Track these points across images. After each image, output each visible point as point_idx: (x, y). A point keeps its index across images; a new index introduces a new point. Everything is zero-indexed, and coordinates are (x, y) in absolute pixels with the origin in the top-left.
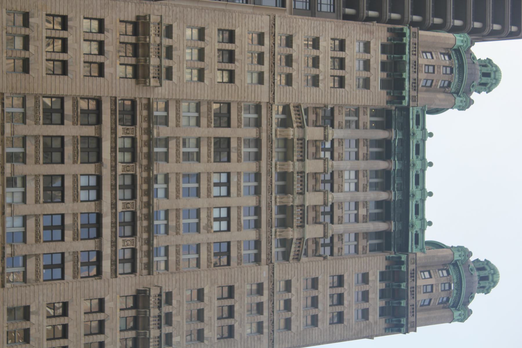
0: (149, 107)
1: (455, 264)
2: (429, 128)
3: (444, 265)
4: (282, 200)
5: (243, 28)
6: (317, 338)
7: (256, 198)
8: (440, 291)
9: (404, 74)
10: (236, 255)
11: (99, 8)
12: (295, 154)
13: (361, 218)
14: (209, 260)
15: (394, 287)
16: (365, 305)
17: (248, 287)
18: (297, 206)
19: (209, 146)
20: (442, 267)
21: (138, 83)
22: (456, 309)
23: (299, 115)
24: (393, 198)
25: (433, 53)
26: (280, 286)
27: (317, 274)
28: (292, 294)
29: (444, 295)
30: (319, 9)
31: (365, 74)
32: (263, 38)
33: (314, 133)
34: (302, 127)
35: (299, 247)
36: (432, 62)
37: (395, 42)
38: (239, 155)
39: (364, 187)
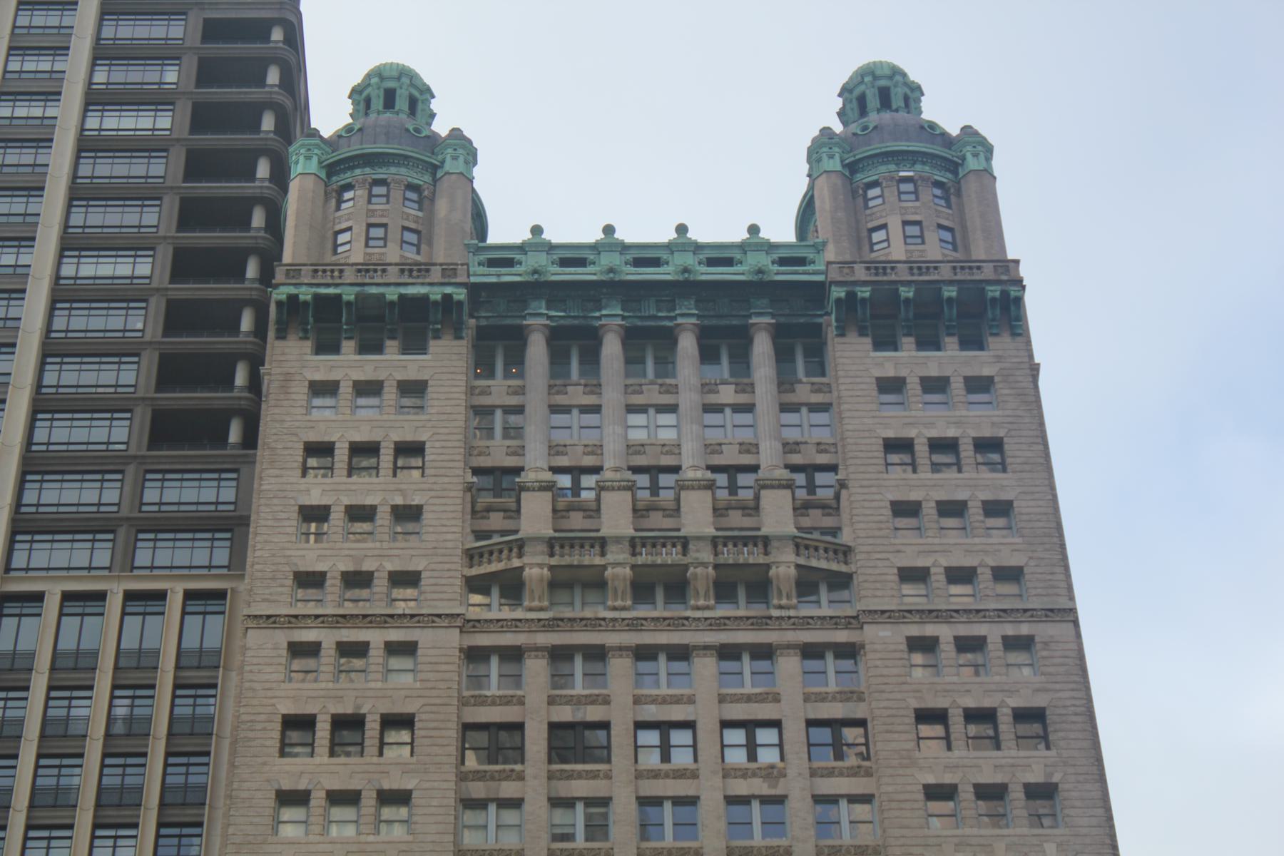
1: (852, 168)
2: (521, 235)
3: (854, 193)
4: (702, 593)
5: (278, 693)
6: (1040, 503)
7: (698, 656)
8: (917, 204)
9: (389, 297)
10: (840, 705)
12: (586, 561)
13: (743, 399)
14: (854, 772)
15: (911, 315)
16: (957, 385)
17: (918, 673)
18: (716, 555)
19: (570, 776)
20: (860, 201)
22: (962, 165)
23: (491, 553)
24: (694, 320)
25: (337, 228)
26: (913, 595)
27: (882, 504)
28: (934, 565)
29: (928, 193)
30: (231, 507)
31: (390, 393)
32: (301, 643)
33: (536, 517)
34: (520, 546)
35: (816, 549)
36: (359, 229)
37: (311, 320)
38: (592, 700)
39: (668, 392)
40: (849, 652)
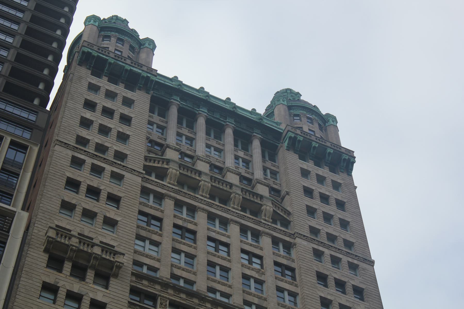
0: (139, 276)
5: (66, 169)
11: (30, 281)
21: (116, 276)
24: (233, 125)
40: (288, 247)
